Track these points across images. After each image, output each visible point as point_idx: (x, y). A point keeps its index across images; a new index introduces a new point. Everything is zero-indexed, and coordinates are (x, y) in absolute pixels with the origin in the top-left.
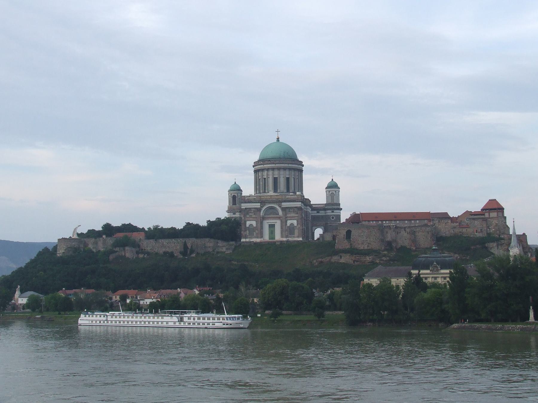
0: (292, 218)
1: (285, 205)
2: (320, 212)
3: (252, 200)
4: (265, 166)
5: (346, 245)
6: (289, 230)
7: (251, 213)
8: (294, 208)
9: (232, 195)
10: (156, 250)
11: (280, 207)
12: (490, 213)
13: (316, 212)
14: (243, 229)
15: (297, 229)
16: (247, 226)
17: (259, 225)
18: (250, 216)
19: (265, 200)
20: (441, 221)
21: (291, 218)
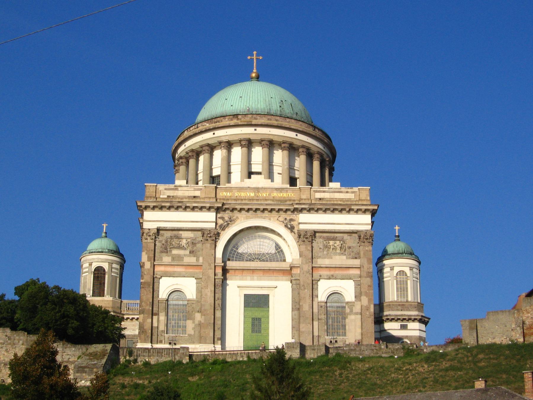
4: (220, 133)
6: (323, 317)
7: (180, 247)
8: (346, 236)
9: (95, 265)
11: (292, 229)
15: (356, 314)
16: (163, 294)
17: (209, 292)
18: (173, 259)
19: (233, 202)
21: (332, 273)
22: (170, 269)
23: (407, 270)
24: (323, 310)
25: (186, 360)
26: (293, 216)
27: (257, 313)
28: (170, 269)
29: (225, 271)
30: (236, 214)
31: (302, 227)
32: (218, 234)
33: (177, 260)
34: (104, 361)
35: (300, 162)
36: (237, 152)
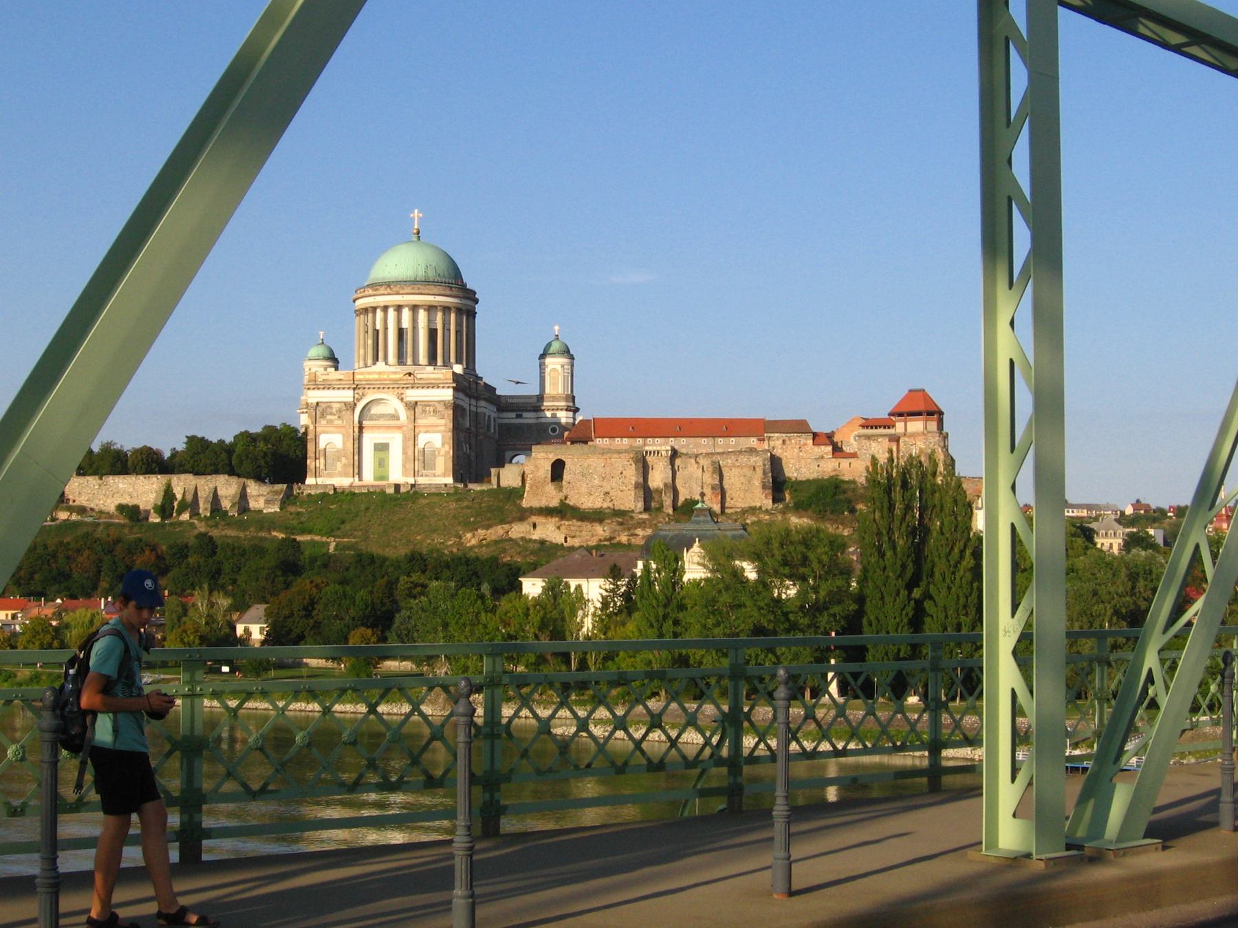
0: (430, 429)
1: (413, 395)
2: (525, 415)
3: (334, 383)
5: (550, 496)
6: (421, 458)
7: (331, 414)
8: (436, 404)
10: (101, 502)
11: (402, 400)
12: (908, 423)
13: (513, 415)
14: (310, 453)
16: (322, 445)
20: (788, 442)
22: (326, 429)
23: (559, 368)
24: (421, 454)
25: (332, 492)
26: (403, 391)
27: (381, 454)
28: (326, 429)
29: (361, 428)
30: (369, 391)
31: (409, 399)
32: (355, 404)
33: (331, 421)
34: (281, 496)
35: (439, 317)
36: (392, 313)
